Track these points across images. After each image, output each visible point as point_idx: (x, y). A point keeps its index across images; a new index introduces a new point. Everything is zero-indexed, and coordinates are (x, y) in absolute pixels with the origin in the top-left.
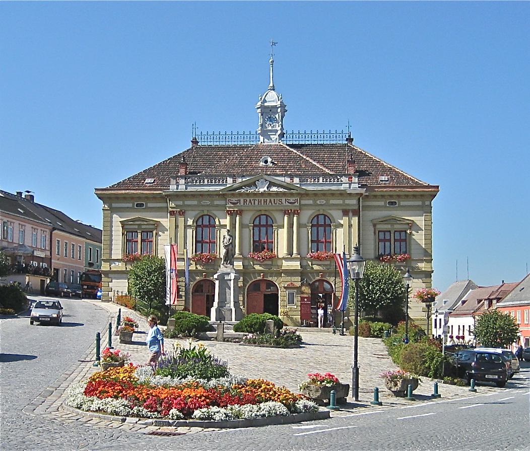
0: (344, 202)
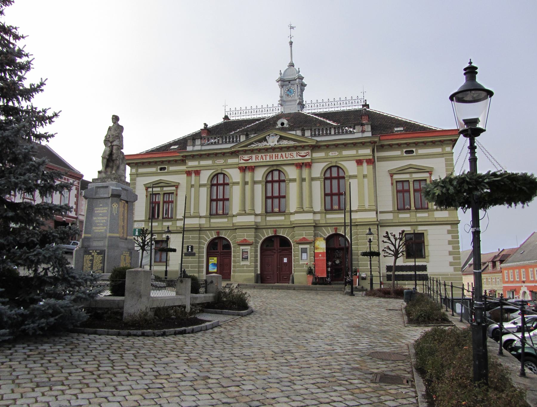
0: (357, 152)
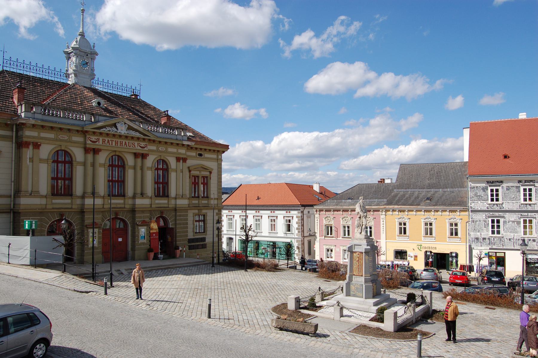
0: (177, 150)
